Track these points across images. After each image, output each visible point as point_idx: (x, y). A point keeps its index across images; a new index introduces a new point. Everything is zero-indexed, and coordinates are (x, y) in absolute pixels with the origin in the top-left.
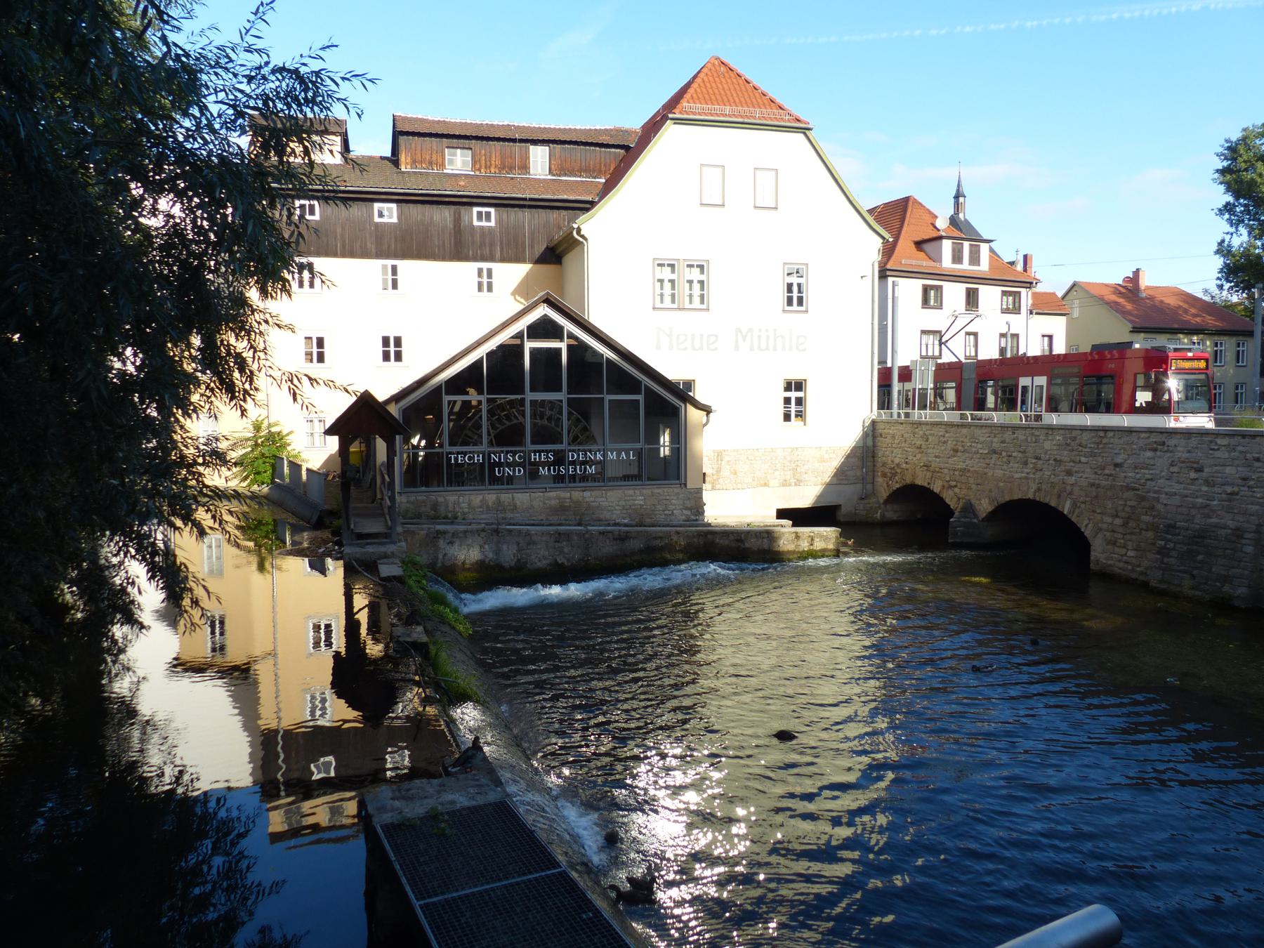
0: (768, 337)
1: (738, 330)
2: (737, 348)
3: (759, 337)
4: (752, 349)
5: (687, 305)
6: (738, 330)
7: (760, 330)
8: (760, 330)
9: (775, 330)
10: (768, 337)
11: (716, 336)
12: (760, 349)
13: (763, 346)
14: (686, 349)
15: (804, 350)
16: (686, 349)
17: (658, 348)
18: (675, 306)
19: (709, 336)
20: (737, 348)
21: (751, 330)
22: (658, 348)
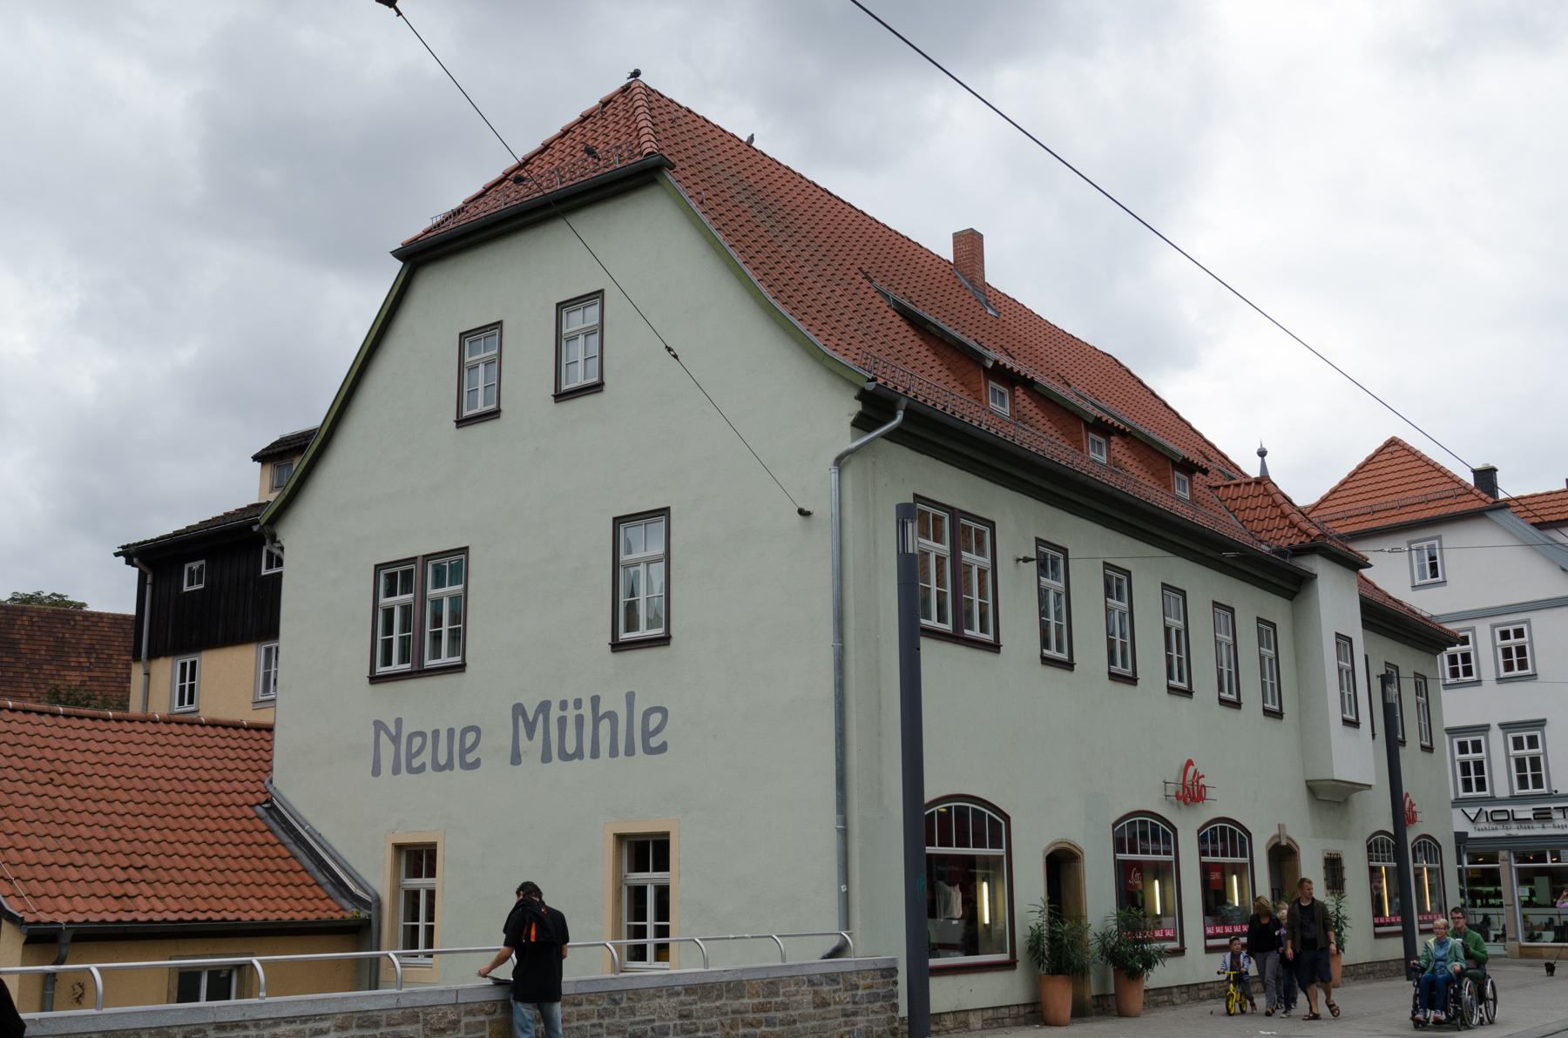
0: (580, 720)
1: (518, 710)
2: (516, 758)
3: (562, 721)
4: (546, 757)
5: (429, 663)
6: (518, 710)
7: (564, 706)
8: (564, 706)
9: (595, 701)
10: (580, 720)
11: (477, 730)
12: (564, 756)
13: (570, 747)
14: (422, 768)
15: (663, 748)
16: (422, 768)
17: (376, 771)
18: (407, 667)
19: (465, 731)
20: (516, 758)
21: (544, 707)
22: (376, 771)
